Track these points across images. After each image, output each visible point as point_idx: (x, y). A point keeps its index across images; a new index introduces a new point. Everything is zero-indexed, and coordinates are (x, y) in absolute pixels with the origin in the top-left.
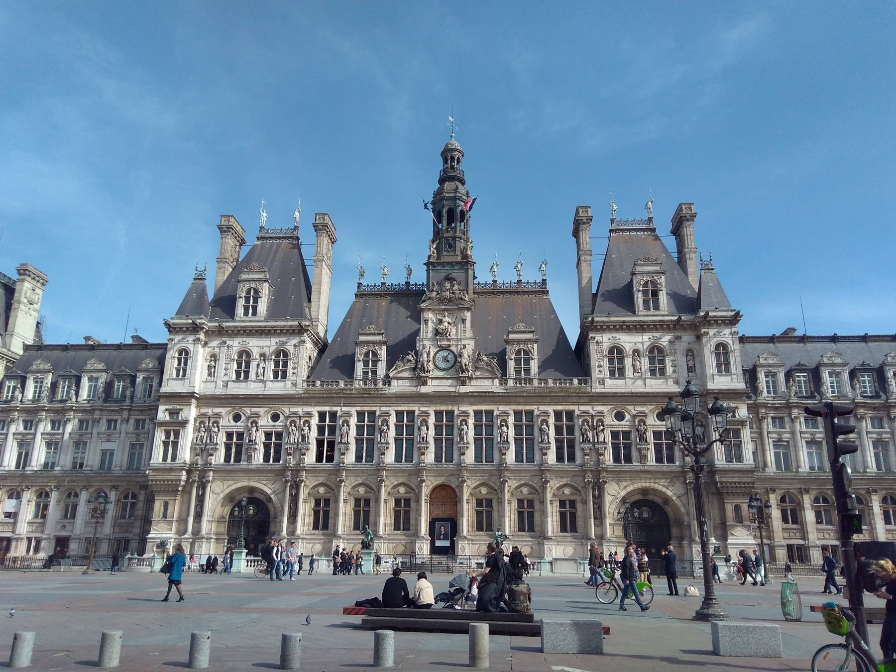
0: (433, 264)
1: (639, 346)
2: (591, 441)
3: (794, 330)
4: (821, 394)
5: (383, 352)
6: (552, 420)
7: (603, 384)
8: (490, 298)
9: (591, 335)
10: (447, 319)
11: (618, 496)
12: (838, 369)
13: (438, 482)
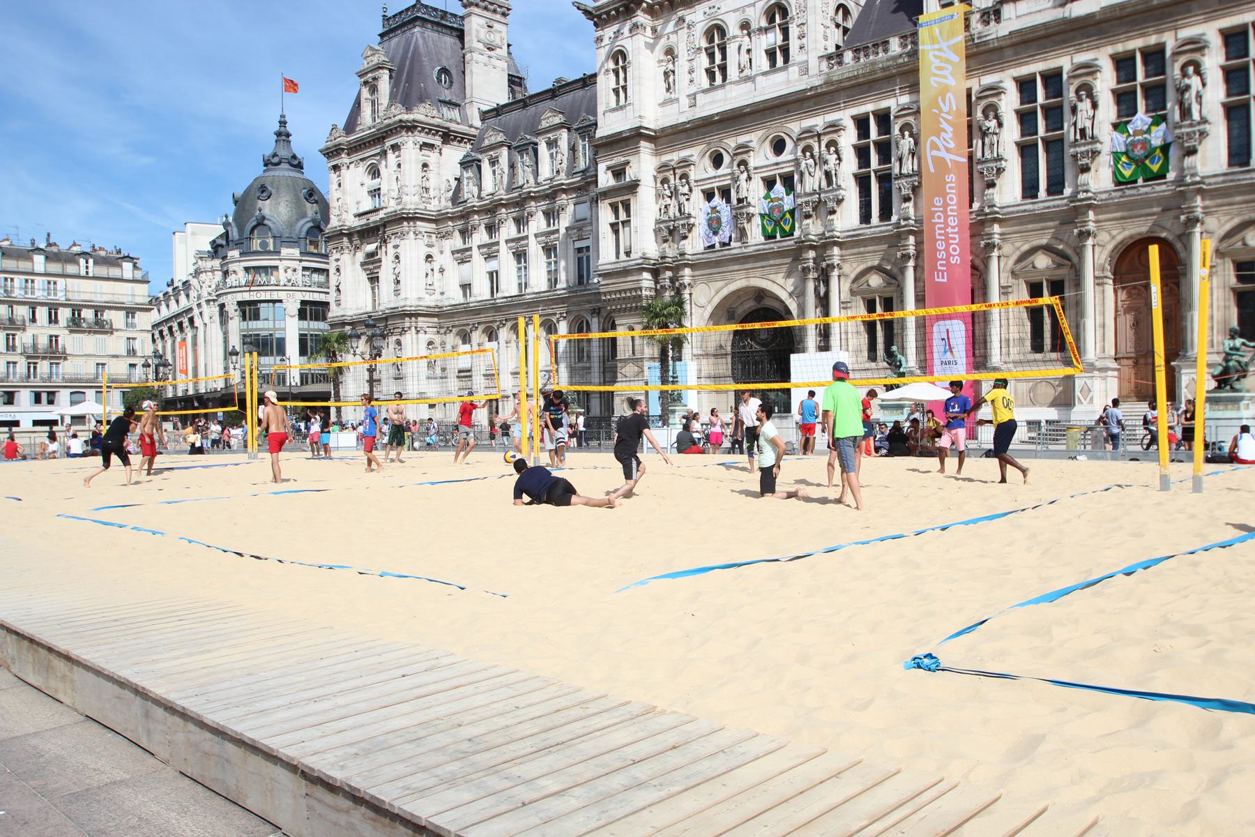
13: (1127, 233)
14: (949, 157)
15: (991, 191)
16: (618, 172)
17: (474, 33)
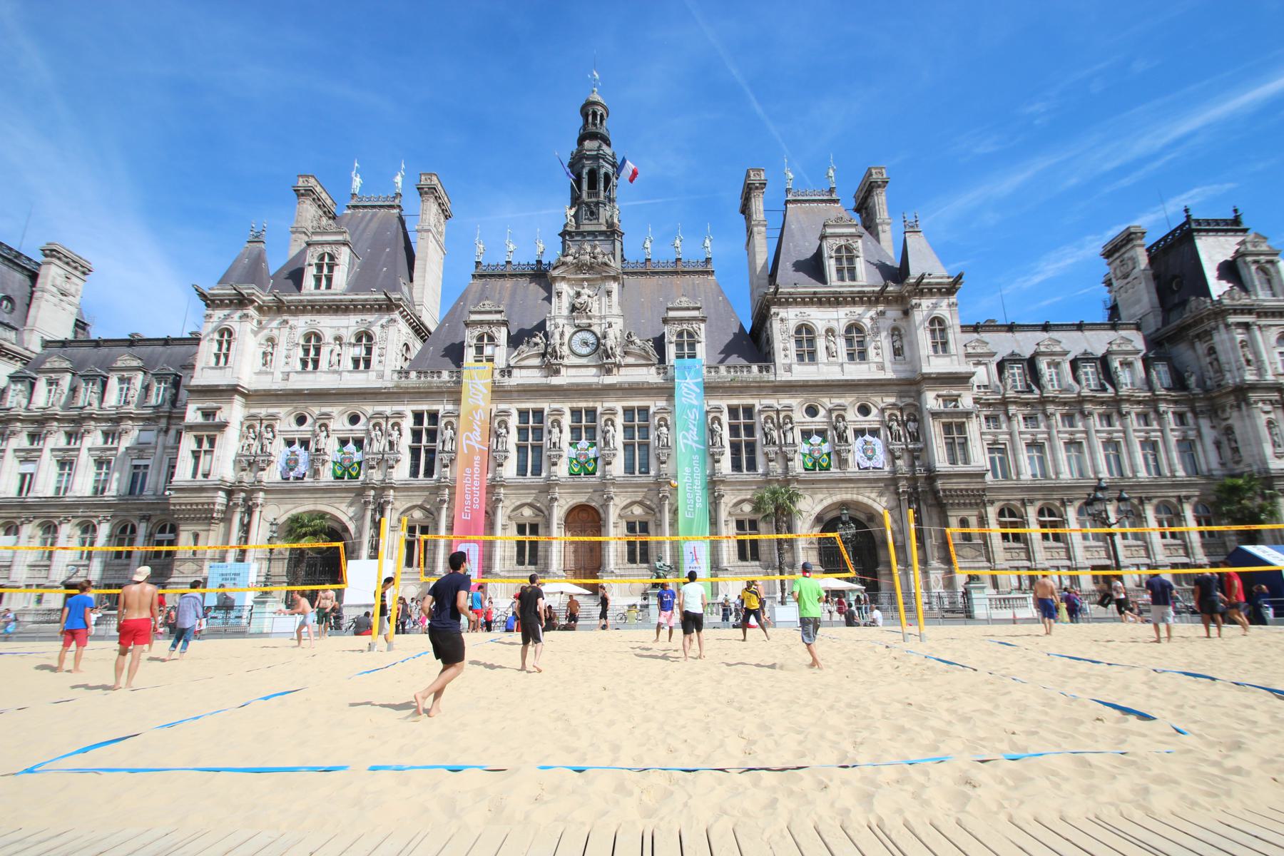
0: (569, 233)
1: (834, 324)
2: (777, 442)
3: (993, 321)
4: (1040, 387)
5: (502, 335)
6: (725, 418)
7: (789, 369)
8: (642, 279)
9: (774, 310)
10: (586, 291)
11: (812, 513)
12: (1058, 359)
13: (575, 501)
14: (477, 446)
15: (500, 468)
16: (208, 414)
17: (50, 278)
